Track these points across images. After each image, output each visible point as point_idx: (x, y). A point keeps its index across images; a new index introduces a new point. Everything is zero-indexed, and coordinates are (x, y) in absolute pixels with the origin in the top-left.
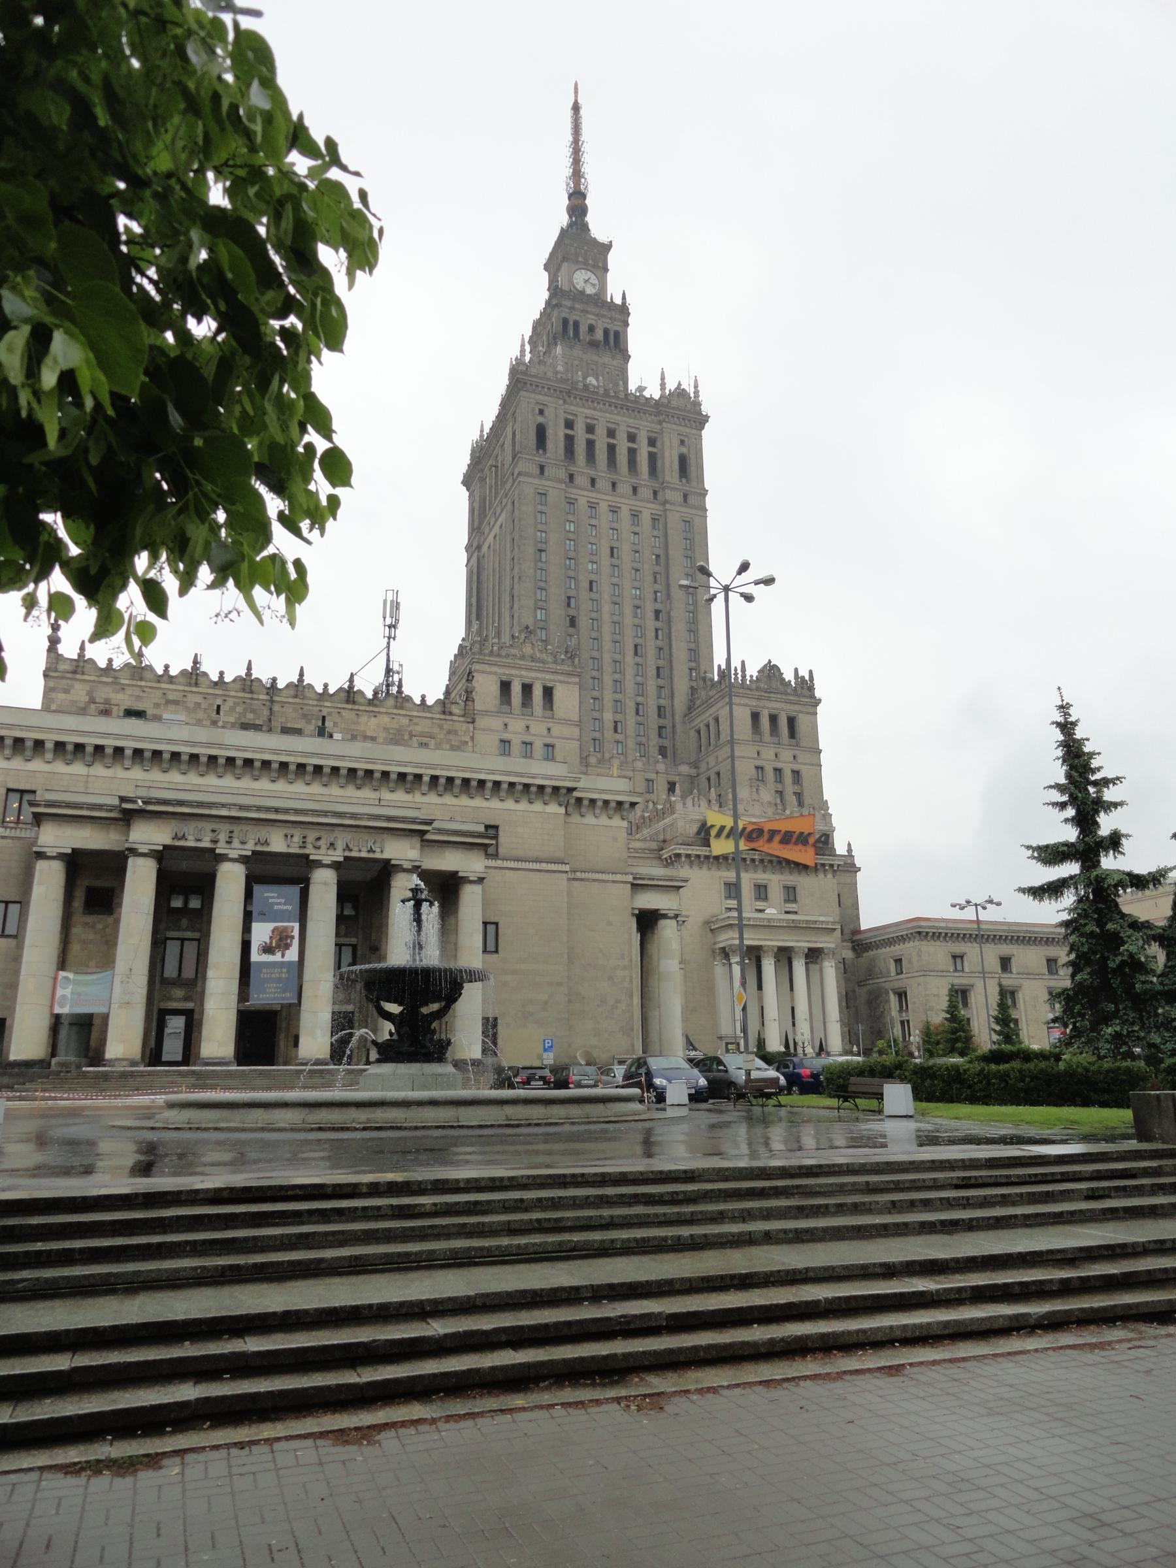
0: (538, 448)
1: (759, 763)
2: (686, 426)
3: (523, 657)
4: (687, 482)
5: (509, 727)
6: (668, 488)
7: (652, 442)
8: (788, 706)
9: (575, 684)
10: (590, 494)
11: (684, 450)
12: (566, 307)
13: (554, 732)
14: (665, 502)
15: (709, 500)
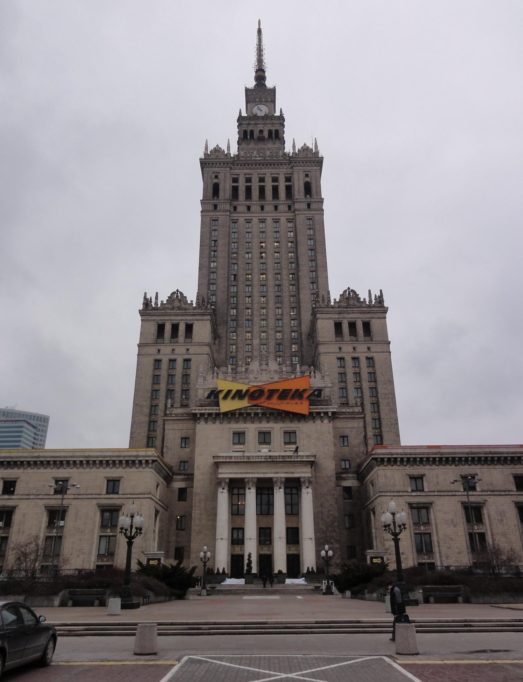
0: (213, 197)
1: (340, 355)
2: (308, 166)
3: (173, 309)
4: (310, 197)
5: (161, 352)
6: (297, 202)
7: (288, 179)
8: (363, 316)
9: (208, 320)
10: (246, 215)
11: (308, 179)
12: (245, 124)
13: (191, 351)
14: (295, 210)
15: (325, 206)
